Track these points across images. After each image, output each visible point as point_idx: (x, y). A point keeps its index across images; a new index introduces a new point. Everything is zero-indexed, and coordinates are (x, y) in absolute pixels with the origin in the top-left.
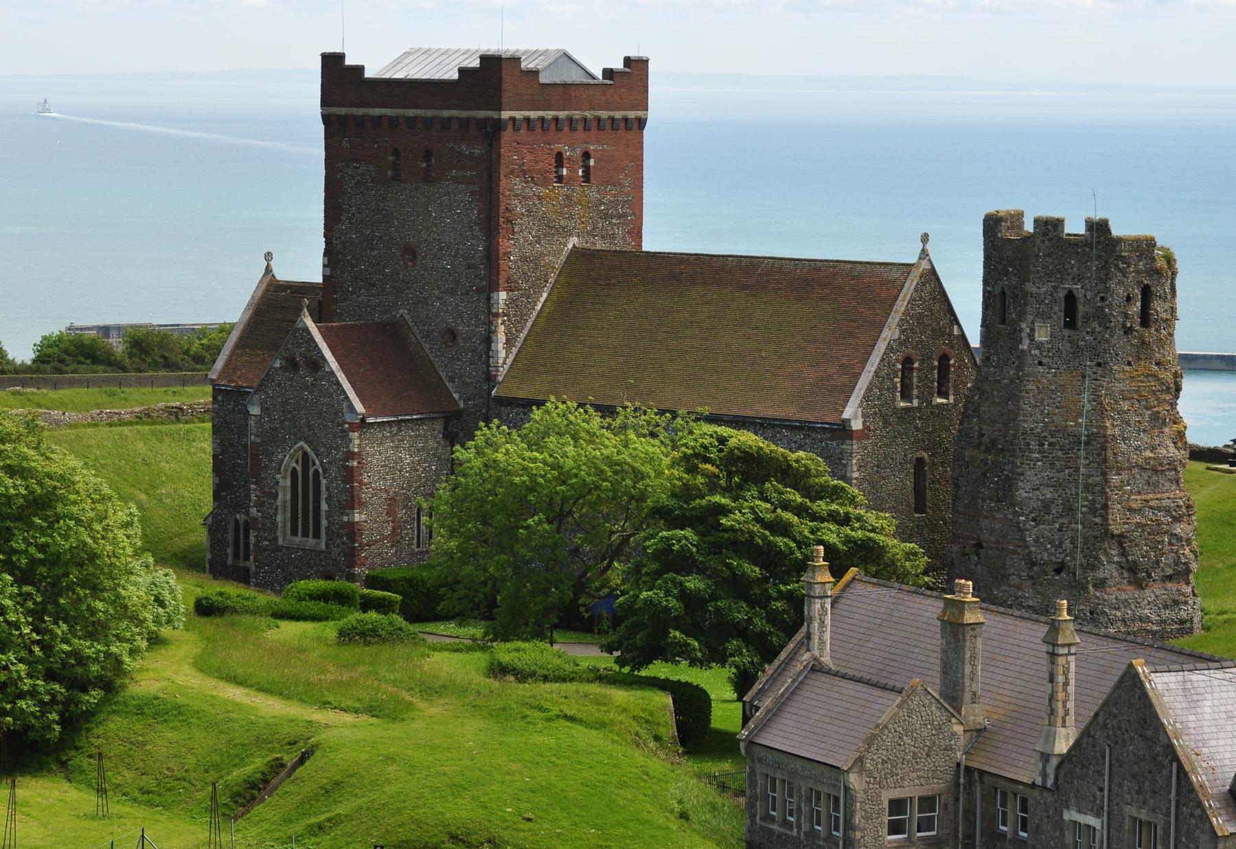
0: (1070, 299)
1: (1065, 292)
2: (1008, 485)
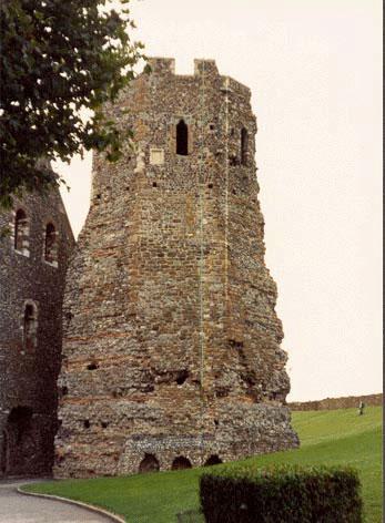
0: (182, 129)
1: (177, 121)
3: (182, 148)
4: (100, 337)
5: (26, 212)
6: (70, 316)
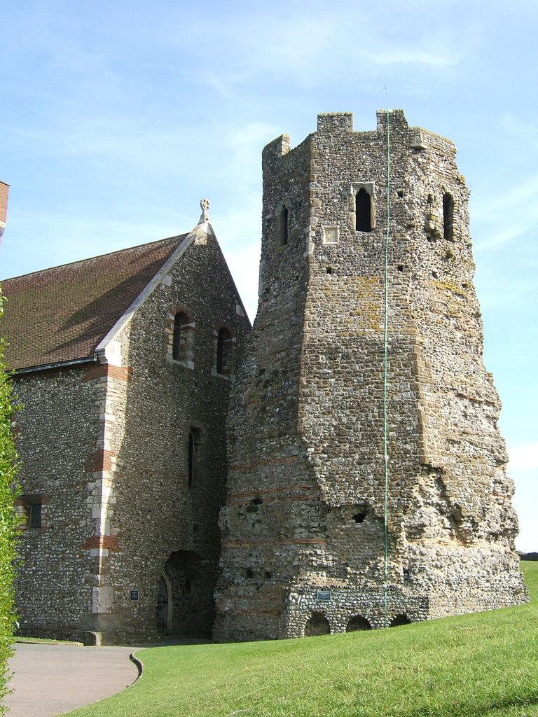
0: (364, 198)
2: (292, 410)
3: (364, 223)
4: (266, 463)
5: (189, 315)
6: (234, 440)
